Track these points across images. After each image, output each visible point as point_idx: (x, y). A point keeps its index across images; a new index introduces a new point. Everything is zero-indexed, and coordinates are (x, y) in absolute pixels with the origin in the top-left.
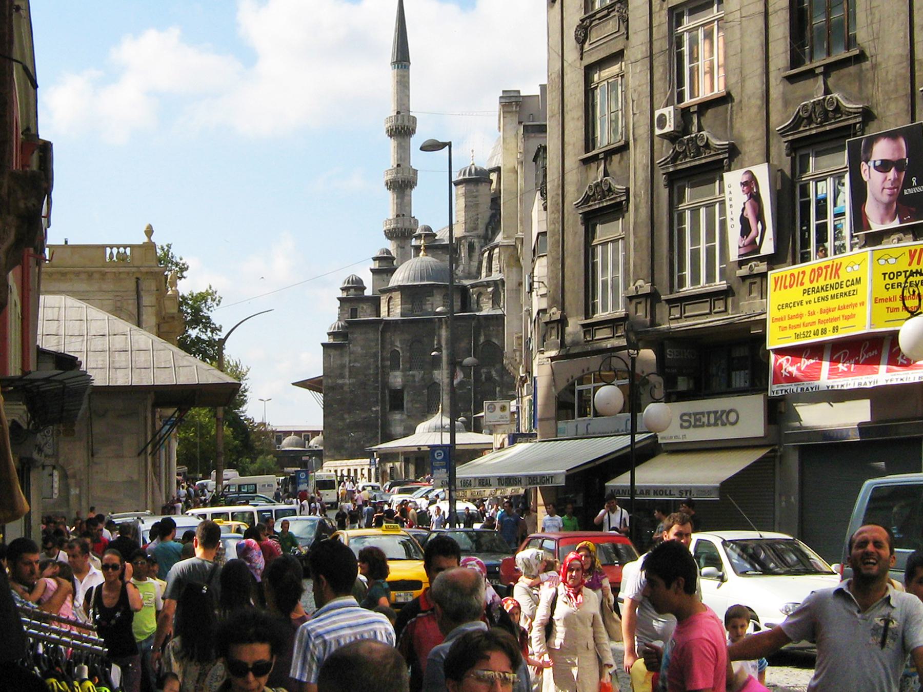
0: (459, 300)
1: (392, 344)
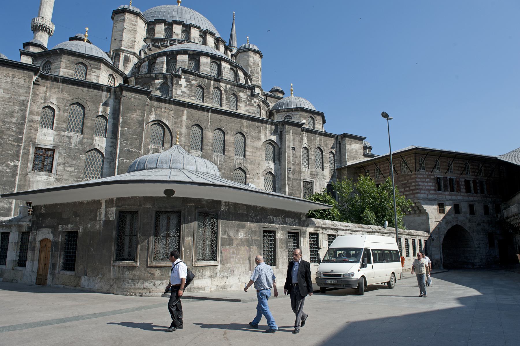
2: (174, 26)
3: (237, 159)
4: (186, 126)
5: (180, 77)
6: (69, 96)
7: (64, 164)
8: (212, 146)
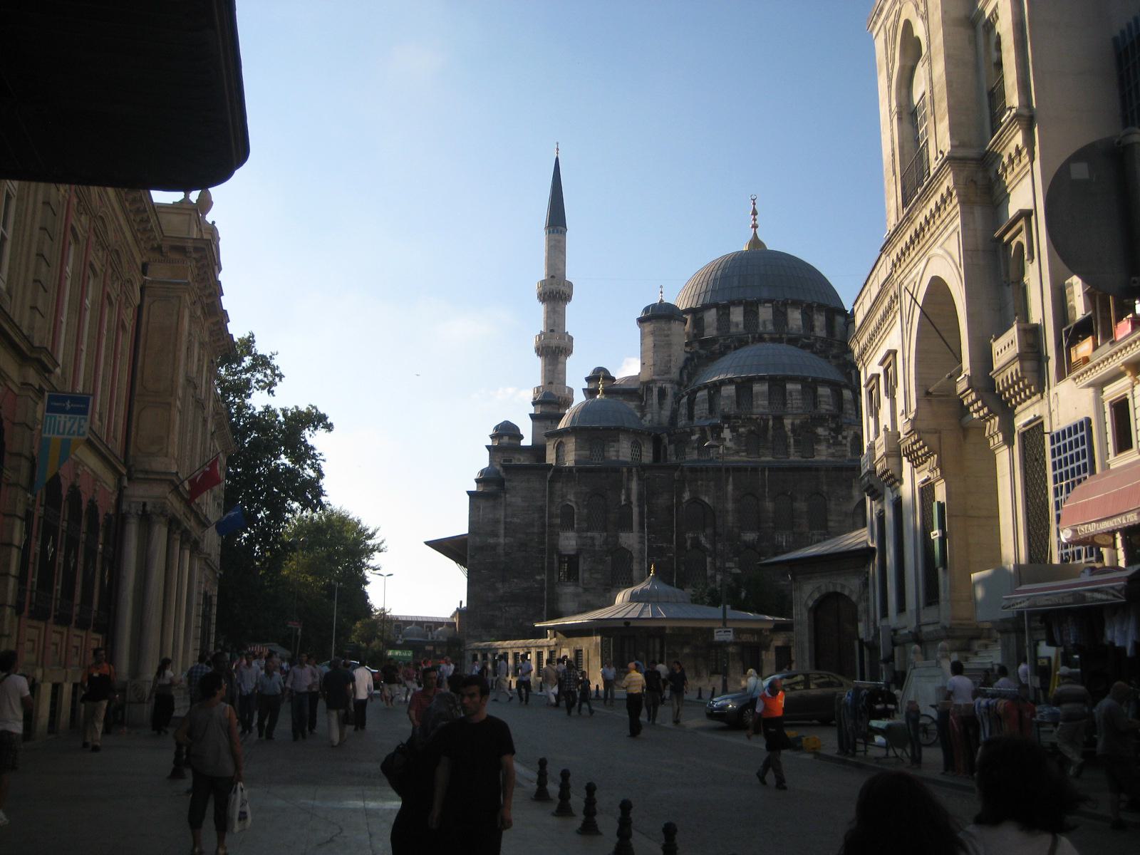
0: (651, 451)
1: (563, 497)
2: (731, 309)
5: (722, 429)
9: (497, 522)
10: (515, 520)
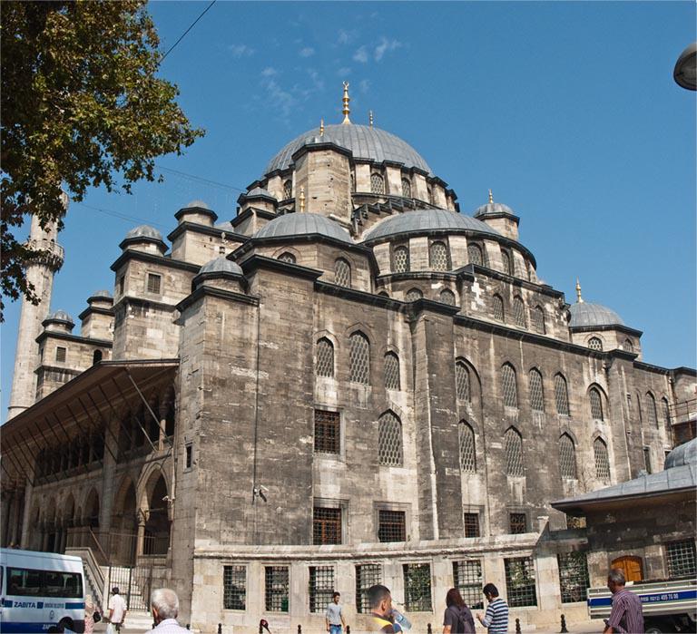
1: (321, 326)
3: (560, 417)
4: (495, 366)
6: (347, 320)
7: (354, 438)
8: (530, 398)
9: (244, 344)
10: (271, 345)
